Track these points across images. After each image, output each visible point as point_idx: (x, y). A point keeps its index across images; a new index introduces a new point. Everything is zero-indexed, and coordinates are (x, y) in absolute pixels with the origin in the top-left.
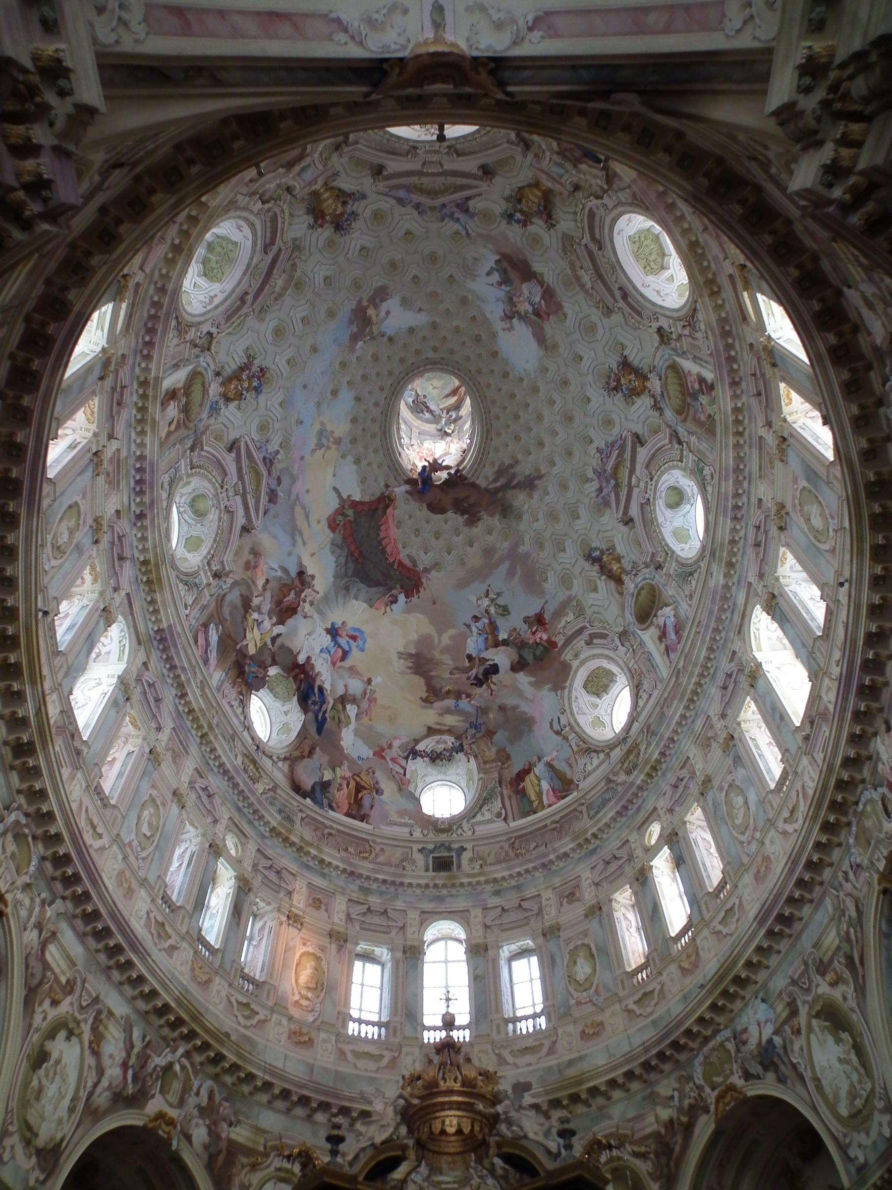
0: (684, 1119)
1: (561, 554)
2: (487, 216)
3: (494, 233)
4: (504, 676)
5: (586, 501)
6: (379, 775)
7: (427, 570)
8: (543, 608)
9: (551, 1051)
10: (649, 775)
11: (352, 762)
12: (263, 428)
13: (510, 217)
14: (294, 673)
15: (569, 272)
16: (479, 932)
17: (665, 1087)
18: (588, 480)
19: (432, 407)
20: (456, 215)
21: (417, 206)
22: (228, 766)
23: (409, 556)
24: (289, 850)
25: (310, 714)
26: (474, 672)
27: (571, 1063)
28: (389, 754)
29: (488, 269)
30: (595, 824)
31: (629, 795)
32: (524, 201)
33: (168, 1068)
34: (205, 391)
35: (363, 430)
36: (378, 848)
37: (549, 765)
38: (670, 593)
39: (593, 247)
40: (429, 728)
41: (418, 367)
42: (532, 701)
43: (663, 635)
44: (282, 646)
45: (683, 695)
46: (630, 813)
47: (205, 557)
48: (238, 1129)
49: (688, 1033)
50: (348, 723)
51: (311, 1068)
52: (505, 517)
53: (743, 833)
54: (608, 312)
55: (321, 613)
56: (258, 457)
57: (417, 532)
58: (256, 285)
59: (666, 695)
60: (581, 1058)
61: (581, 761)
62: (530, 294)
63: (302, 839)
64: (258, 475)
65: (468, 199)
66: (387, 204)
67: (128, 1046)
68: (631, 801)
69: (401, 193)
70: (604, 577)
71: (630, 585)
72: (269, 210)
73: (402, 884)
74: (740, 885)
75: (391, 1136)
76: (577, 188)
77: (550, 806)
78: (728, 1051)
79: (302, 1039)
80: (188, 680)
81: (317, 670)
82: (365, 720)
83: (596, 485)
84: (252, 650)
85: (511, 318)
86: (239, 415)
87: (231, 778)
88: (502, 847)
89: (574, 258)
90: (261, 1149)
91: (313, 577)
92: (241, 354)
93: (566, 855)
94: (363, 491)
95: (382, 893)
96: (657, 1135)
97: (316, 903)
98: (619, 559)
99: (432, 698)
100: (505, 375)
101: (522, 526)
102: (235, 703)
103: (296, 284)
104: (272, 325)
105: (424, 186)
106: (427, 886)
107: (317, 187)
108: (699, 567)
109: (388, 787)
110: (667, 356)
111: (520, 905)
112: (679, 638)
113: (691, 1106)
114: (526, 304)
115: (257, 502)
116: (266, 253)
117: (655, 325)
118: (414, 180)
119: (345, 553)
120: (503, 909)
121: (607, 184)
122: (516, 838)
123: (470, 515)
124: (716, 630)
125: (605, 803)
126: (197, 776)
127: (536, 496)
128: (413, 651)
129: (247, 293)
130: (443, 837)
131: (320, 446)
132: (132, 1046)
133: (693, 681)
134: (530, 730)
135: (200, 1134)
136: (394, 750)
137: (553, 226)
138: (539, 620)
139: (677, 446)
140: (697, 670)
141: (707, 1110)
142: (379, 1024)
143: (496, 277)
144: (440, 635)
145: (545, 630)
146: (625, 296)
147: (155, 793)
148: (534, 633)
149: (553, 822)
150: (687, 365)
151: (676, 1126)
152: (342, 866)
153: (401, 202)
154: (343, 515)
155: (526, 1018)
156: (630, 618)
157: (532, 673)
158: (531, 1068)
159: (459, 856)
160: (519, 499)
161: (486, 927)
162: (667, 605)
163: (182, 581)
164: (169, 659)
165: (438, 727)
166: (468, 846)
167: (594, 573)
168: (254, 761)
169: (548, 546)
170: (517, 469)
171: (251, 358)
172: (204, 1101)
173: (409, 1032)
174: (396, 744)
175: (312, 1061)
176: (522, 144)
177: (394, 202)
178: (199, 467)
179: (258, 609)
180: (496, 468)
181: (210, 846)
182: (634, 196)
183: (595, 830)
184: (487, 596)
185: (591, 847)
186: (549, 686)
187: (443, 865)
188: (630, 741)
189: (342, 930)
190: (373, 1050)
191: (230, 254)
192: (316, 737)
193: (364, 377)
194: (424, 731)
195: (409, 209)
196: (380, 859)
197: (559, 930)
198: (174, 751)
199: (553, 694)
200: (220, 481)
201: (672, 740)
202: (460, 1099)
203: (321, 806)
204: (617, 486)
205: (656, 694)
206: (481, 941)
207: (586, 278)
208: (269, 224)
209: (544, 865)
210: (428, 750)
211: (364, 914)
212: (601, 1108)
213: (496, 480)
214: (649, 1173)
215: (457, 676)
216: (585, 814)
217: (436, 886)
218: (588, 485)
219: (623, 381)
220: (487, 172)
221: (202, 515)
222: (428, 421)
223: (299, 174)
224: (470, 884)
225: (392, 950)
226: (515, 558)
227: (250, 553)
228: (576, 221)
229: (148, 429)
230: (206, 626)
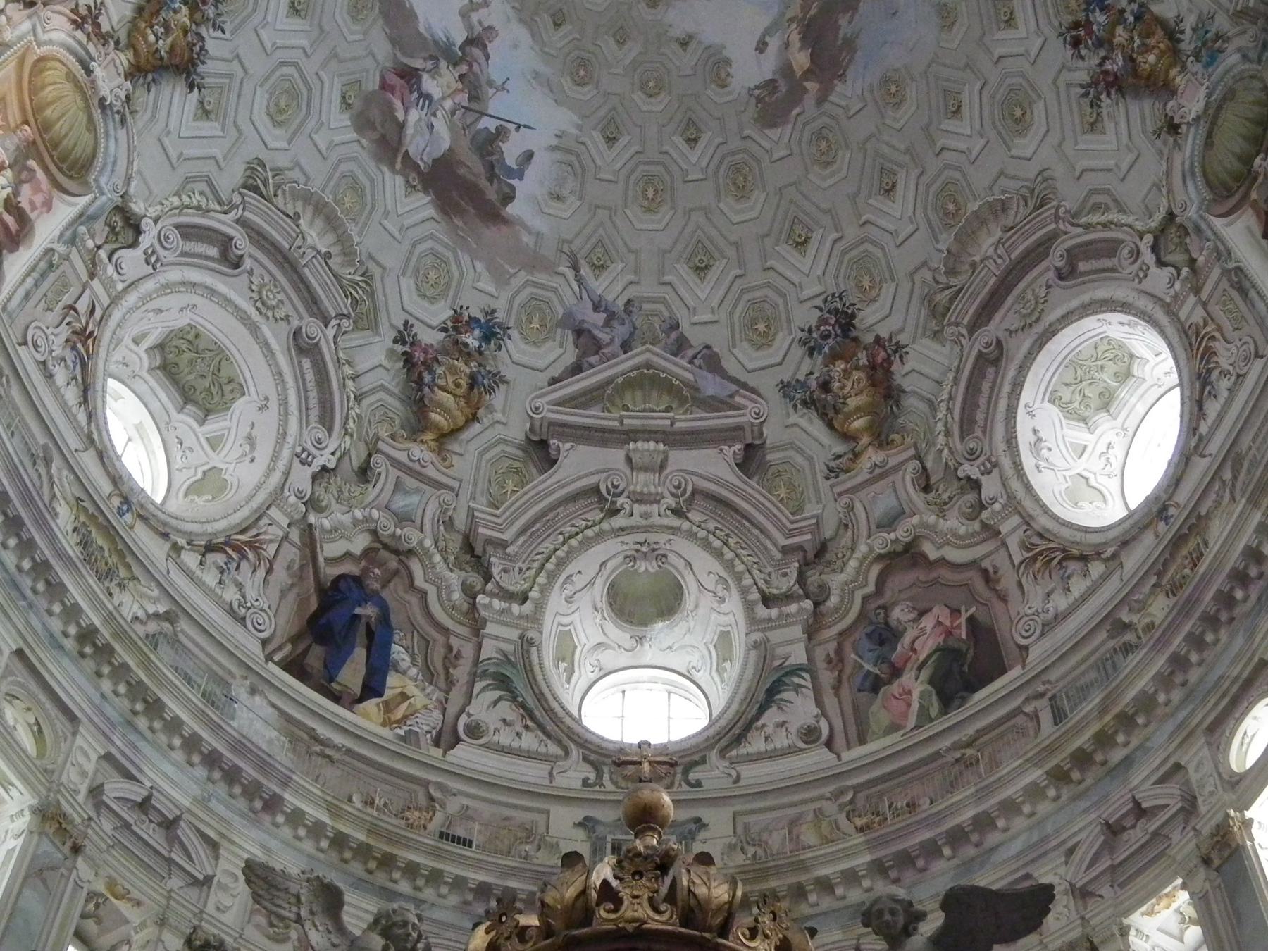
3: (523, 276)
13: (492, 332)
15: (352, 229)
20: (600, 318)
21: (680, 345)
29: (530, 172)
32: (464, 382)
39: (312, 327)
65: (576, 369)
69: (711, 386)
72: (972, 455)
76: (364, 473)
85: (470, 42)
89: (345, 272)
92: (1109, 125)
105: (666, 400)
107: (872, 457)
114: (436, 93)
118: (685, 421)
121: (310, 526)
137: (400, 340)
143: (511, 151)
153: (712, 362)
182: (255, 546)
195: (697, 337)
207: (315, 236)
208: (980, 416)
223: (902, 513)
228: (354, 378)
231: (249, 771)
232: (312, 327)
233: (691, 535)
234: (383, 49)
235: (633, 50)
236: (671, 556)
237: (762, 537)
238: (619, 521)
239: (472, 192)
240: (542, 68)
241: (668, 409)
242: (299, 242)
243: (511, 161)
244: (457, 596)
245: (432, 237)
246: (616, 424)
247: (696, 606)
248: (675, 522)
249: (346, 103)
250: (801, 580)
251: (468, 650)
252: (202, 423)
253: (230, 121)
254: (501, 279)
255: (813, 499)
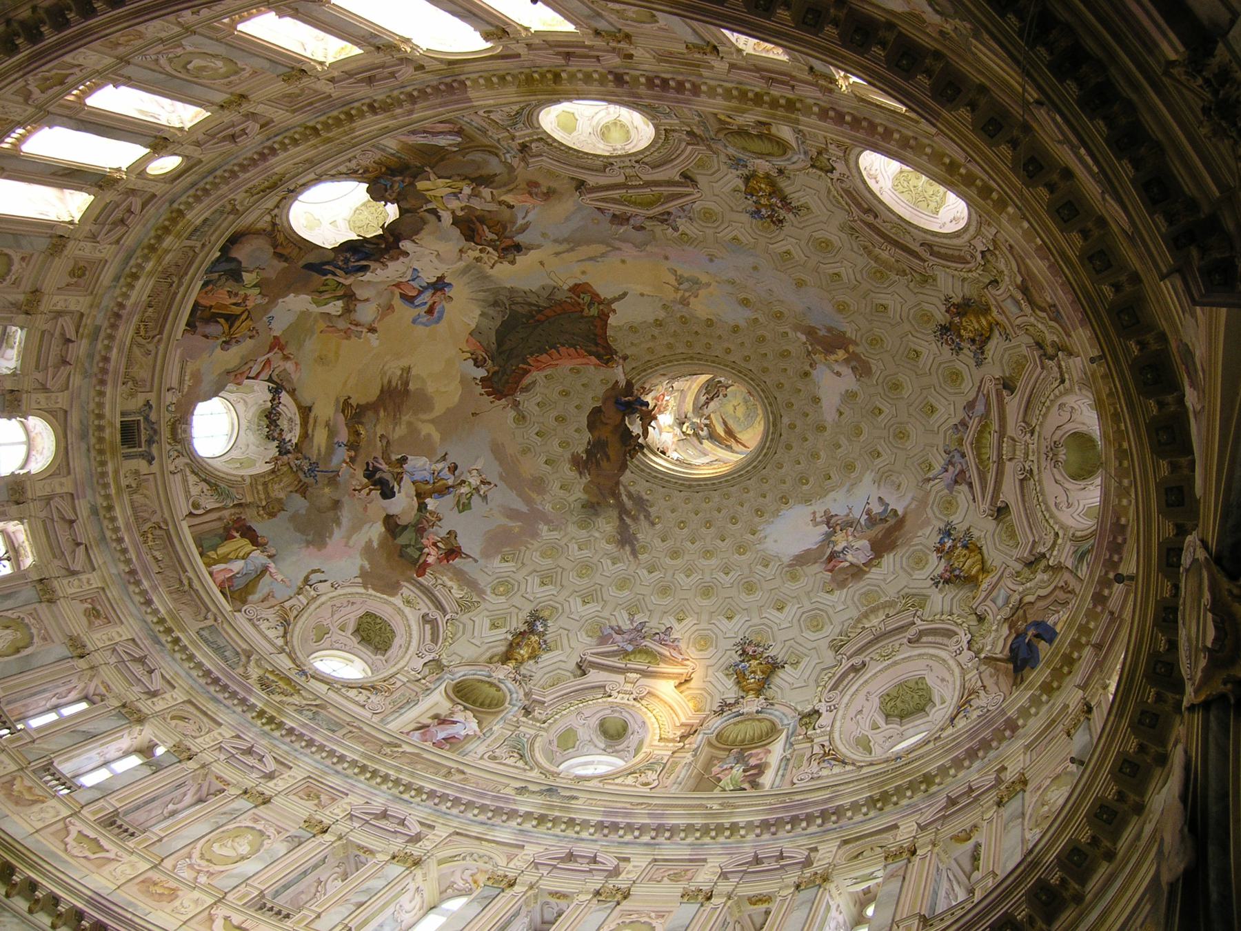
1: (537, 581)
2: (949, 505)
3: (928, 510)
4: (379, 506)
5: (606, 614)
6: (248, 344)
7: (516, 405)
8: (468, 556)
10: (261, 714)
11: (265, 309)
12: (708, 216)
13: (947, 531)
14: (387, 235)
15: (882, 600)
16: (41, 490)
18: (631, 616)
19: (712, 405)
20: (951, 468)
21: (964, 424)
22: (273, 160)
23: (534, 383)
24: (152, 233)
25: (332, 255)
26: (384, 466)
28: (275, 356)
30: (193, 642)
31: (234, 687)
32: (965, 552)
34: (761, 155)
35: (696, 333)
36: (151, 347)
37: (265, 570)
38: (495, 728)
39: (913, 631)
40: (310, 409)
41: (770, 404)
42: (346, 545)
43: (442, 721)
44: (424, 222)
45: (371, 758)
46: (212, 689)
47: (549, 136)
50: (318, 304)
52: (583, 507)
53: (202, 857)
54: (836, 647)
55: (466, 270)
56: (672, 206)
57: (564, 393)
58: (885, 228)
59: (366, 729)
61: (271, 614)
62: (856, 549)
63: (167, 251)
64: (650, 204)
65: (970, 485)
66: (968, 388)
68: (225, 688)
69: (980, 408)
70: (510, 637)
71: (502, 673)
72: (972, 256)
73: (103, 382)
74: (134, 858)
76: (981, 619)
77: (211, 574)
80: (394, 117)
81: (390, 264)
82: (322, 325)
83: (626, 626)
84: (421, 185)
85: (828, 524)
86: (727, 189)
87: (254, 162)
88: (154, 512)
89: (899, 607)
91: (513, 262)
92: (803, 201)
93: (149, 602)
94: (620, 328)
95: (91, 356)
97: (79, 271)
98: (534, 656)
99: (349, 412)
100: (759, 512)
101: (572, 529)
102: (353, 165)
103: (880, 272)
104: (834, 239)
106: (100, 416)
108: (532, 769)
109: (232, 356)
110: (786, 722)
111: (78, 544)
112: (438, 745)
114: (844, 544)
115: (614, 201)
116: (922, 245)
117: (822, 708)
119: (543, 303)
120: (72, 522)
121: (985, 658)
122: (167, 531)
123: (586, 462)
124: (456, 801)
125: (219, 650)
126: (262, 121)
127: (611, 548)
128: (411, 387)
129: (876, 216)
130: (165, 433)
131: (680, 280)
133: (391, 772)
134: (308, 543)
136: (281, 363)
137: (936, 584)
138: (453, 552)
139: (679, 733)
140: (405, 778)
143: (877, 509)
144: (432, 421)
145: (440, 560)
146: (855, 669)
147: (246, 74)
148: (435, 544)
149: (190, 579)
150: (777, 749)
152: (129, 303)
153: (970, 406)
154: (591, 304)
156: (461, 673)
157: (382, 544)
159: (142, 455)
160: (606, 525)
161: (48, 499)
162: (480, 723)
163: (523, 109)
164: (423, 94)
165: (311, 421)
166: (155, 467)
167: (514, 625)
168: (274, 186)
169: (547, 563)
170: (644, 523)
171: (796, 210)
174: (289, 366)
176: (1033, 559)
177: (971, 397)
178: (667, 138)
179: (475, 194)
180: (646, 497)
181: (166, 139)
182: (973, 692)
183: (185, 641)
184: (482, 482)
185: (163, 638)
186: (367, 566)
187: (129, 433)
188: (301, 680)
189: (42, 308)
191: (925, 204)
192: (302, 263)
193: (762, 340)
194: (306, 401)
195: (961, 414)
196: (137, 351)
197: (50, 601)
198: (299, 95)
199: (357, 573)
200: (646, 160)
201: (310, 743)
203: (210, 271)
204: (625, 654)
205: (366, 714)
206: (29, 495)
207: (875, 621)
208: (956, 253)
209: (132, 572)
210: (281, 408)
211: (63, 334)
213: (630, 496)
215: (379, 444)
216: (202, 625)
217: (100, 428)
218: (626, 616)
219: (754, 663)
220: (1001, 512)
221: (603, 134)
222: (697, 398)
224: (103, 475)
225: (14, 374)
226: (531, 520)
227: (549, 188)
229: (734, 103)
230: (460, 132)
231: (986, 733)
232: (913, 631)
233: (1041, 425)
234: (817, 568)
235: (843, 441)
236: (1056, 438)
237: (1040, 381)
238: (1035, 471)
239: (890, 532)
240: (845, 489)
241: (990, 433)
242: (874, 629)
243: (880, 509)
244: (1046, 577)
245: (902, 557)
246: (995, 465)
247: (1084, 424)
248: (1036, 434)
249: (830, 592)
250: (1052, 358)
251: (1067, 576)
252: (935, 705)
253: (806, 651)
254: (927, 522)
255: (1019, 349)
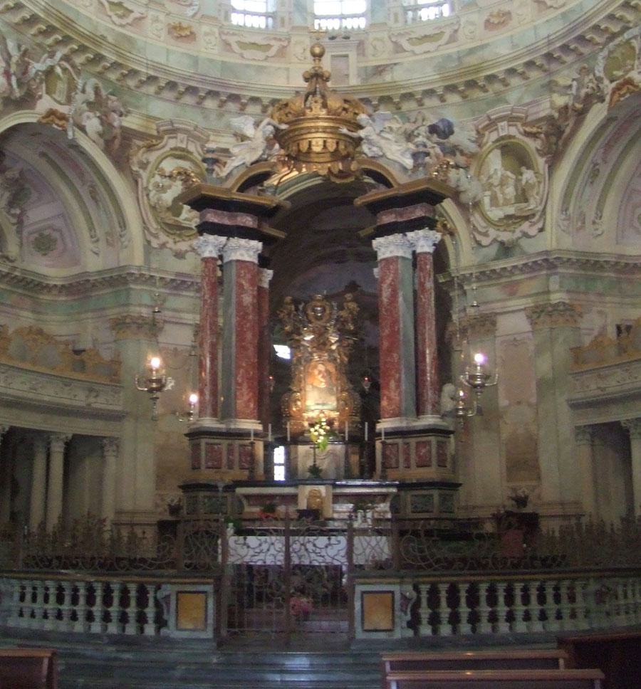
0: (579, 106)
9: (453, 39)
17: (565, 77)
27: (471, 51)
33: (50, 72)
48: (129, 118)
49: (596, 28)
51: (195, 61)
60: (482, 47)
67: (6, 56)
75: (261, 156)
78: (633, 48)
79: (183, 34)
90: (155, 133)
96: (550, 119)
113: (588, 96)
132: (10, 56)
135: (93, 124)
141: (602, 100)
142: (267, 15)
151: (570, 111)
155: (428, 6)
158: (428, 56)
172: (92, 97)
173: (298, 20)
175: (195, 54)
190: (259, 40)
202: (326, 124)
212: (497, 93)
214: (538, 150)
